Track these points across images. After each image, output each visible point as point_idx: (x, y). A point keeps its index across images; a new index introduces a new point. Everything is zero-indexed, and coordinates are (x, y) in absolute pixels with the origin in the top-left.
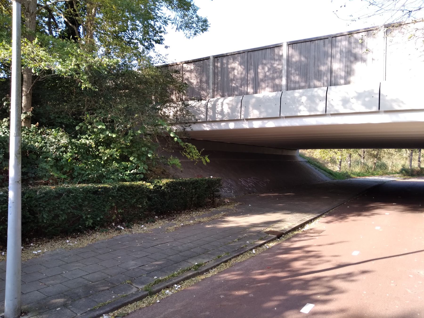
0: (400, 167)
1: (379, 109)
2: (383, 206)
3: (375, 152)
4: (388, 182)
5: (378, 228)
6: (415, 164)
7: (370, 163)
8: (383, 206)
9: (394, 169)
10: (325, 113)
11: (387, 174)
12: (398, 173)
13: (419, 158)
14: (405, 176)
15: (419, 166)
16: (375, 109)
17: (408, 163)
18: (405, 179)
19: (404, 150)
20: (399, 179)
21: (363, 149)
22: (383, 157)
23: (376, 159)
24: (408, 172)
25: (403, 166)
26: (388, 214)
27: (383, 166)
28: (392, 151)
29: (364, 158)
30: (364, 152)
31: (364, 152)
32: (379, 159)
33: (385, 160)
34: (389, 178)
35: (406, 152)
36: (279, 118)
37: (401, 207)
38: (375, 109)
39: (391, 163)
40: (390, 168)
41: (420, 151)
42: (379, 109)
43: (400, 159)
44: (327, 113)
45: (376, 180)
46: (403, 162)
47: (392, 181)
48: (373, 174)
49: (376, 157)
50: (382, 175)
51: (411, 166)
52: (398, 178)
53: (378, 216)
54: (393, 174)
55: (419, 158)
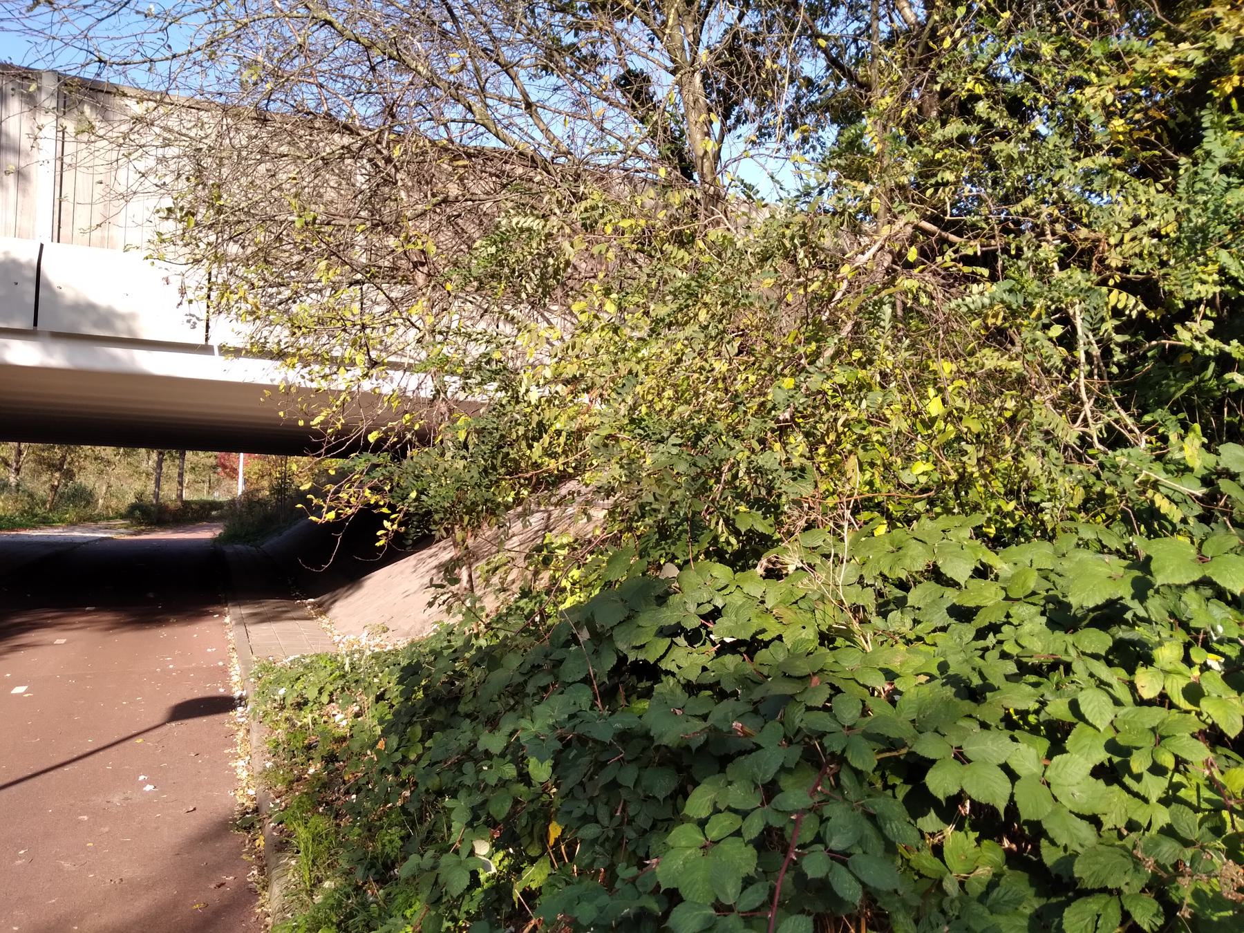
0: (131, 499)
1: (35, 324)
2: (52, 618)
3: (58, 452)
4: (87, 543)
5: (19, 690)
6: (169, 492)
7: (42, 485)
8: (52, 618)
9: (114, 503)
10: (203, 342)
11: (91, 519)
12: (123, 517)
13: (181, 475)
14: (140, 524)
15: (156, 495)
16: (24, 323)
17: (151, 486)
18: (139, 533)
19: (143, 450)
20: (121, 534)
21: (16, 444)
22: (80, 469)
23: (57, 475)
24: (148, 513)
25: (139, 496)
26: (63, 641)
27: (83, 497)
28: (107, 452)
29: (18, 470)
30: (20, 453)
31: (20, 453)
32: (69, 475)
33: (87, 478)
34: (94, 531)
35: (146, 459)
36: (205, 349)
37: (108, 617)
38: (24, 323)
39: (104, 488)
40: (101, 501)
41: (183, 455)
42: (35, 324)
43: (131, 476)
44: (39, 328)
45: (52, 540)
46: (138, 486)
47: (89, 542)
48: (46, 522)
49: (59, 470)
50: (72, 524)
51: (156, 495)
52: (122, 530)
53: (31, 651)
54: (108, 519)
55: (181, 475)
